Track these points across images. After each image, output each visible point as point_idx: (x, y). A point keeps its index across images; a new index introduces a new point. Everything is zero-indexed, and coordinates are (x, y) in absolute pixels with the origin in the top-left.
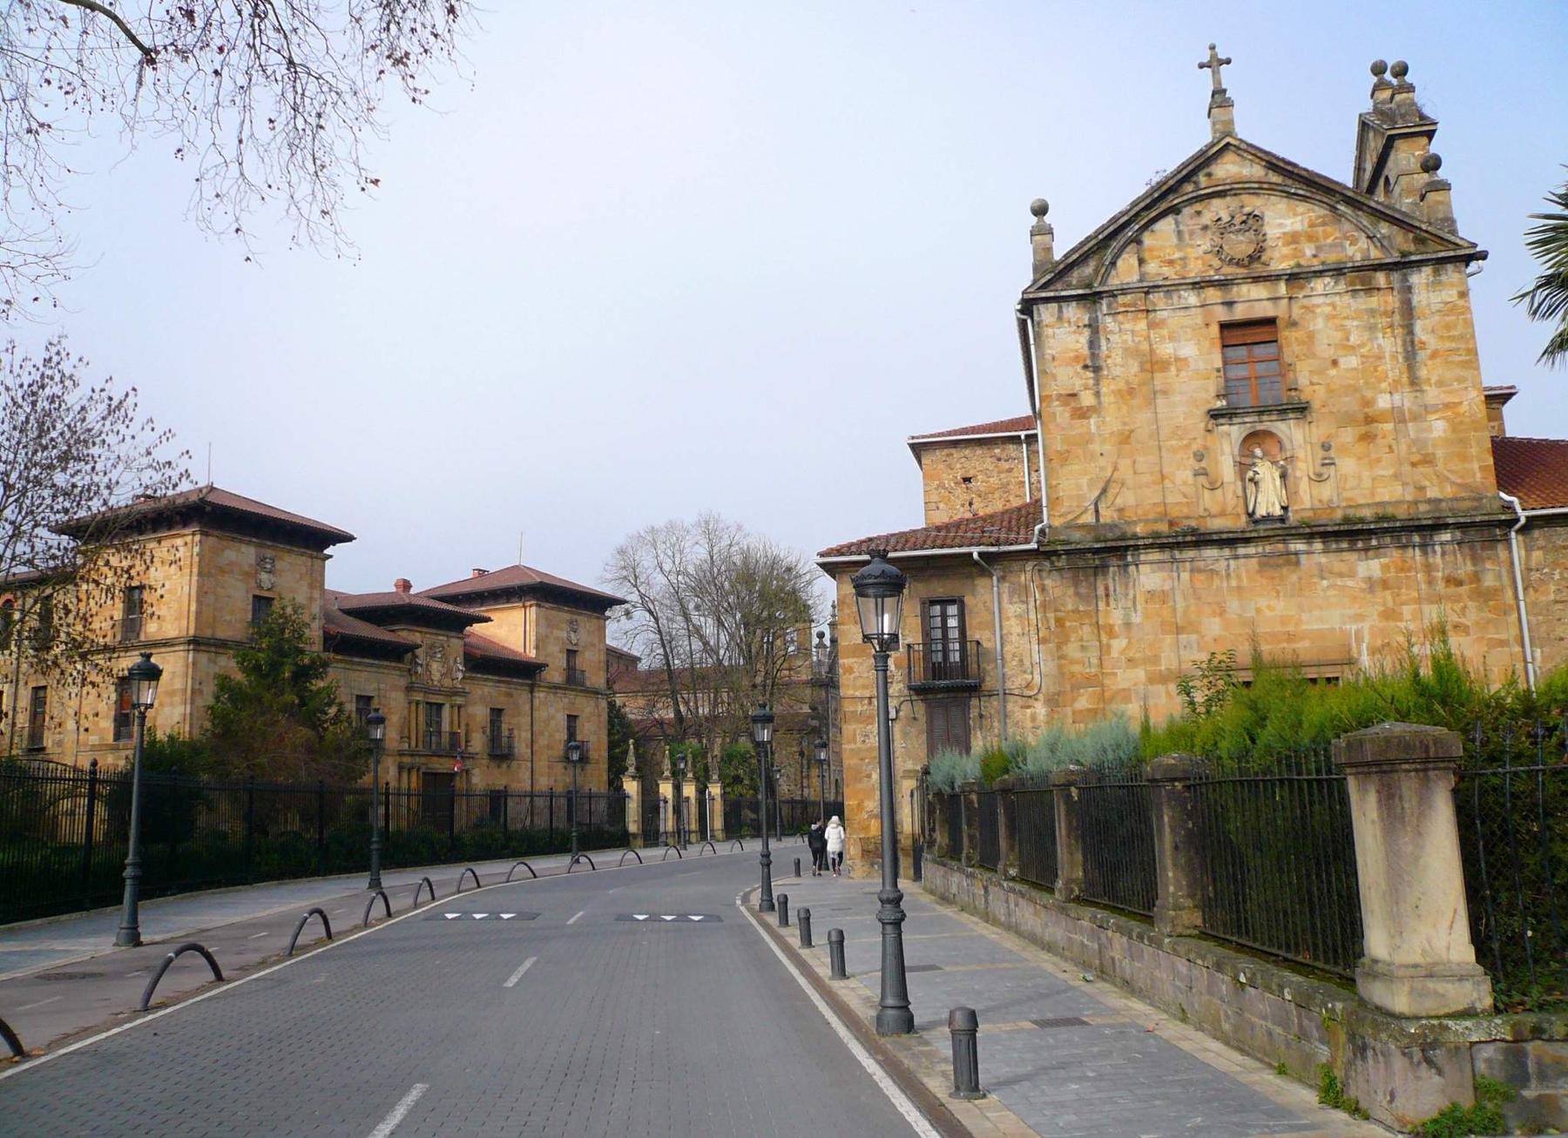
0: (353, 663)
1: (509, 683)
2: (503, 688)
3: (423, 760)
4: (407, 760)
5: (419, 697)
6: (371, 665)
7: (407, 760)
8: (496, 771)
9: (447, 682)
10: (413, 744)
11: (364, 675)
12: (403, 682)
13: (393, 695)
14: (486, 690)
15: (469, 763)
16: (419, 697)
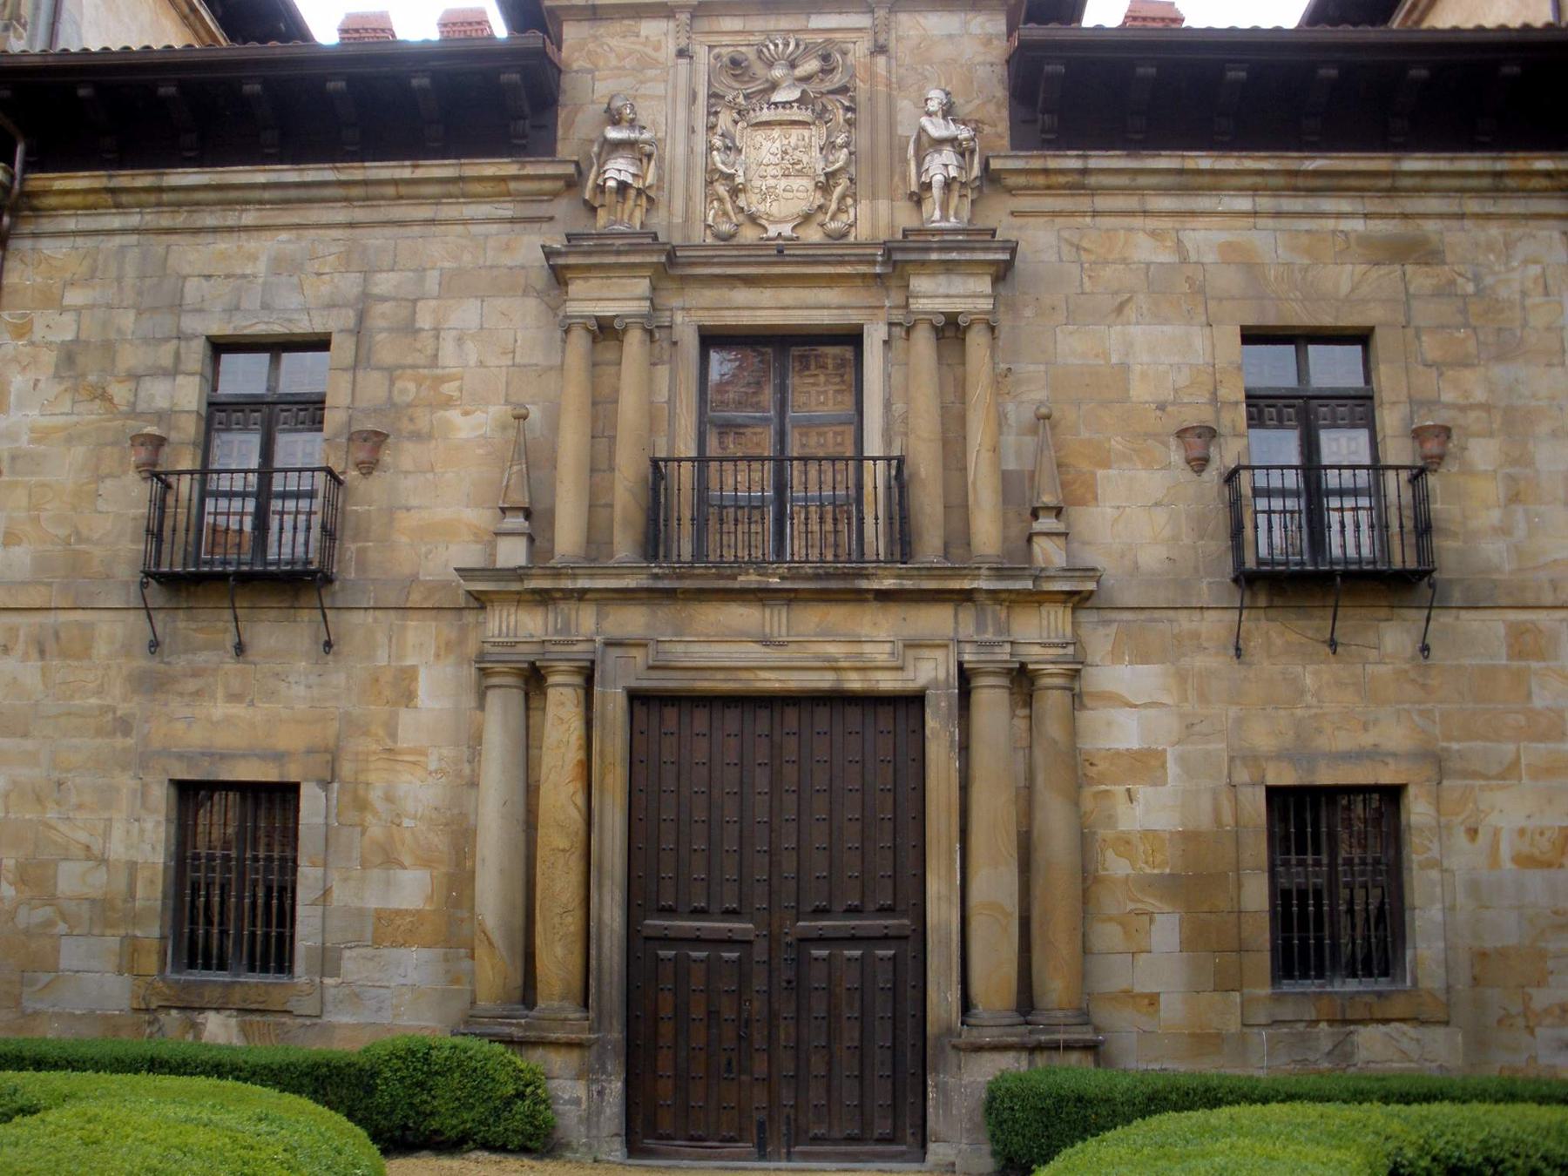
0: (188, 199)
1: (1391, 186)
2: (1348, 219)
3: (632, 621)
4: (528, 626)
5: (620, 298)
6: (306, 195)
7: (528, 626)
8: (1312, 676)
9: (872, 219)
10: (567, 537)
11: (265, 247)
12: (529, 248)
13: (466, 314)
14: (1204, 239)
15: (1037, 634)
16: (620, 298)
